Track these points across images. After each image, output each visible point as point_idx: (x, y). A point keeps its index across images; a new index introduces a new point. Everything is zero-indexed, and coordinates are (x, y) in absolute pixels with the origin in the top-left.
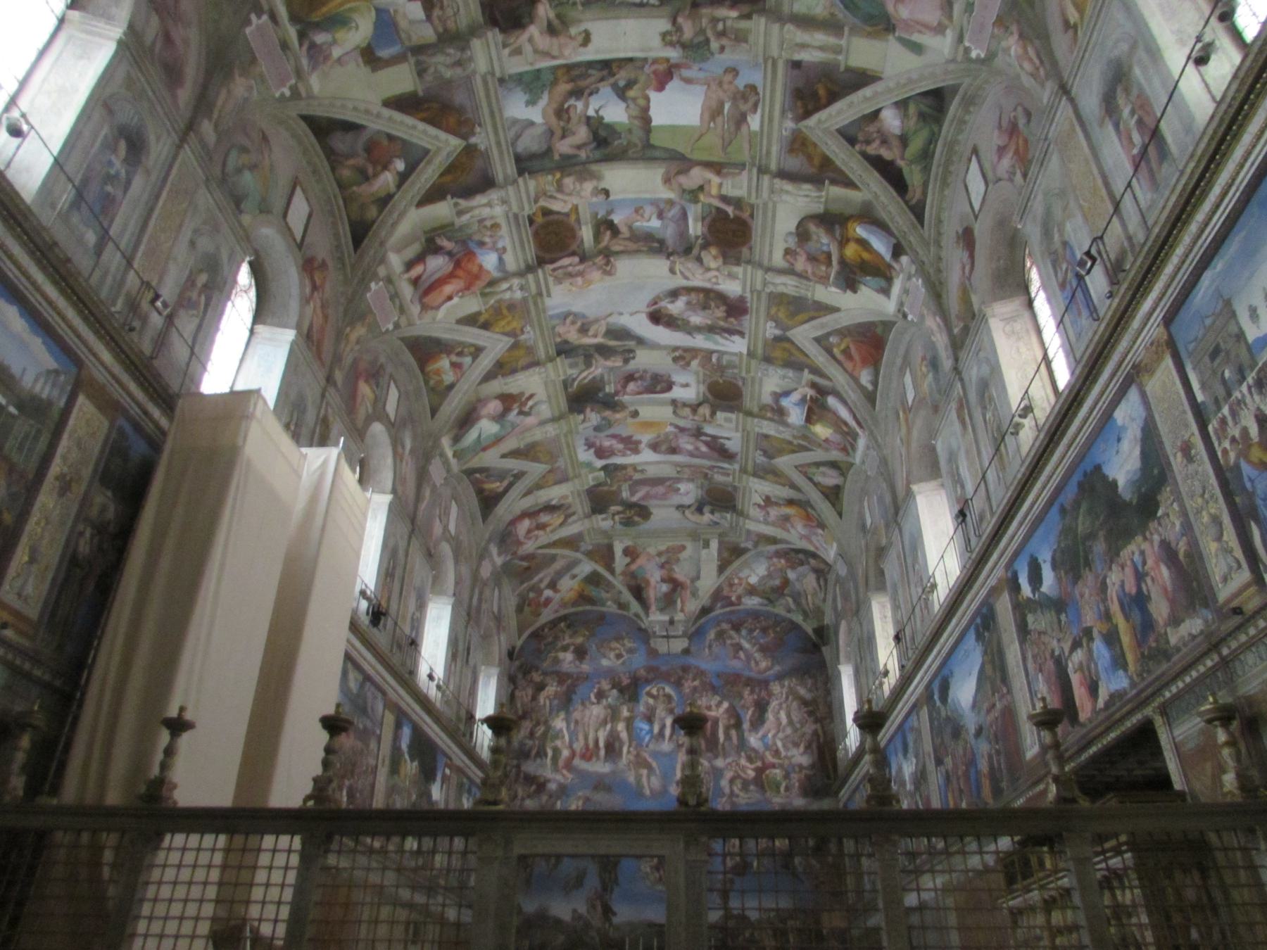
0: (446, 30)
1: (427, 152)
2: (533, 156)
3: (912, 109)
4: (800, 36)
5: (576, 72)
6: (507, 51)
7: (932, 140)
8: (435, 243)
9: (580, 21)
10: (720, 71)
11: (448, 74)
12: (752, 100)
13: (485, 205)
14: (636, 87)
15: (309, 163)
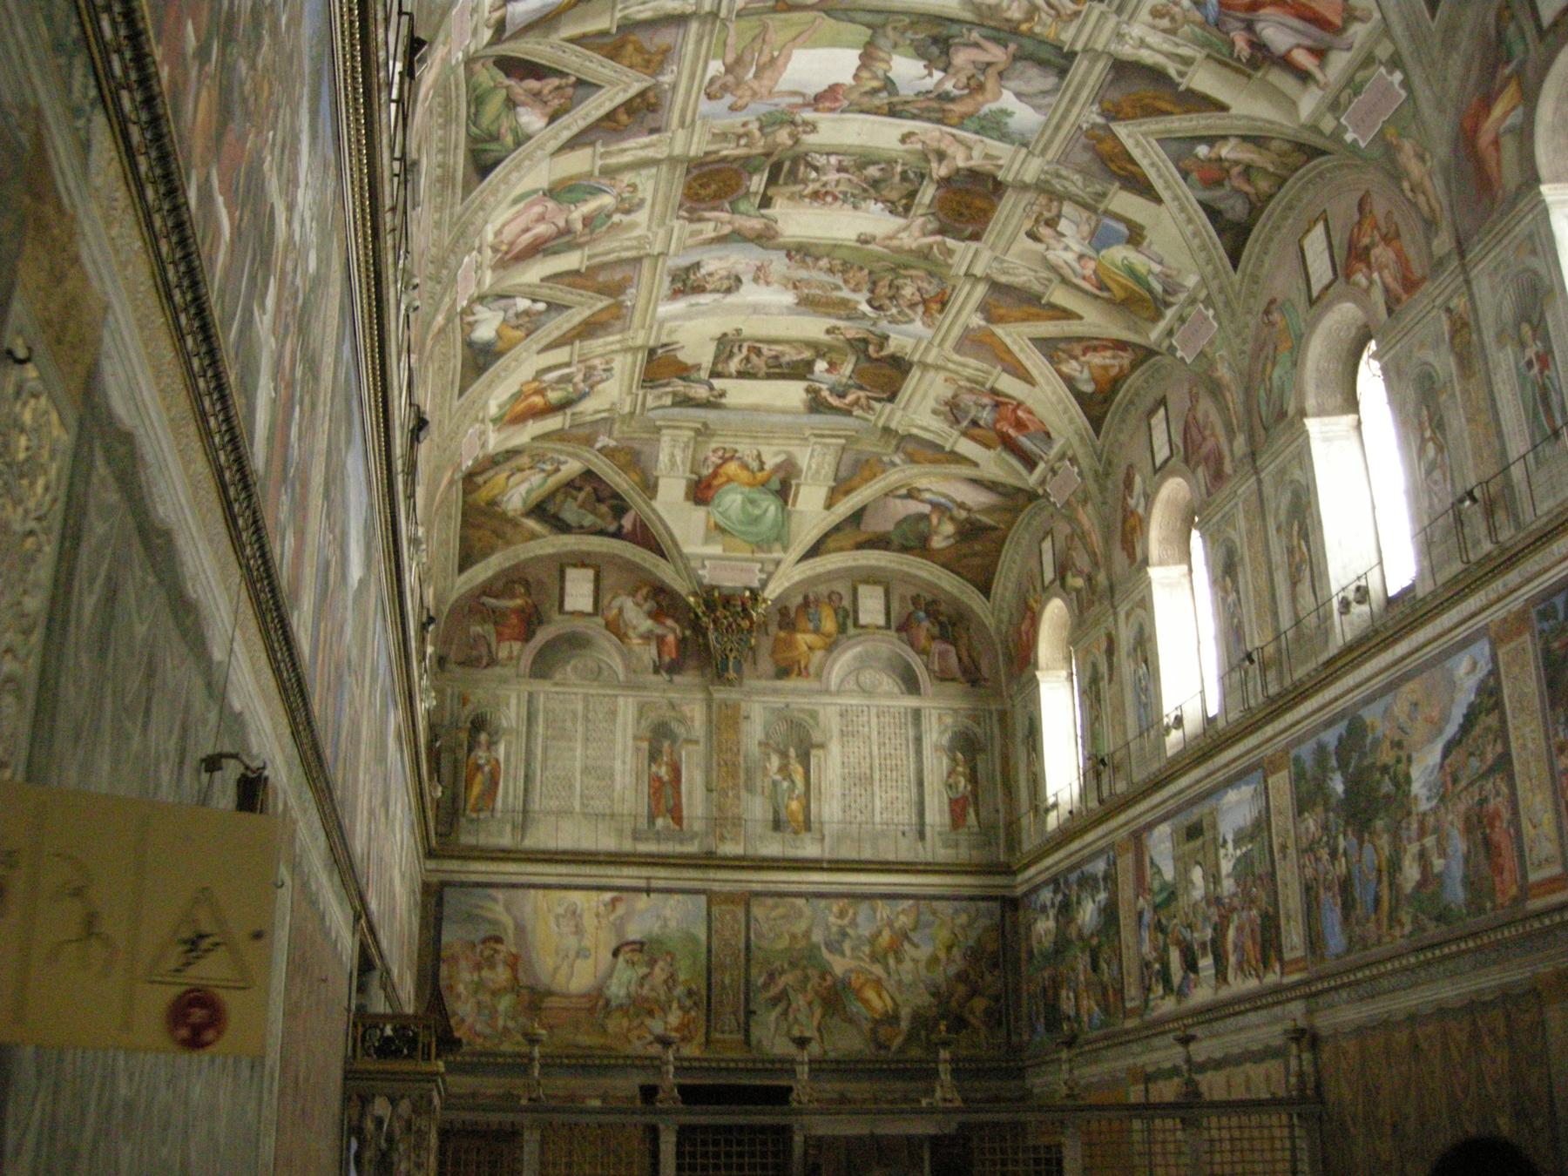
0: (1051, 200)
1: (1158, 140)
2: (1042, 63)
3: (509, 139)
4: (651, 153)
5: (934, 115)
6: (1001, 162)
7: (474, 119)
8: (1252, 55)
9: (906, 151)
10: (752, 106)
11: (1076, 177)
12: (716, 86)
13: (1149, 47)
14: (867, 88)
15: (1285, 218)
